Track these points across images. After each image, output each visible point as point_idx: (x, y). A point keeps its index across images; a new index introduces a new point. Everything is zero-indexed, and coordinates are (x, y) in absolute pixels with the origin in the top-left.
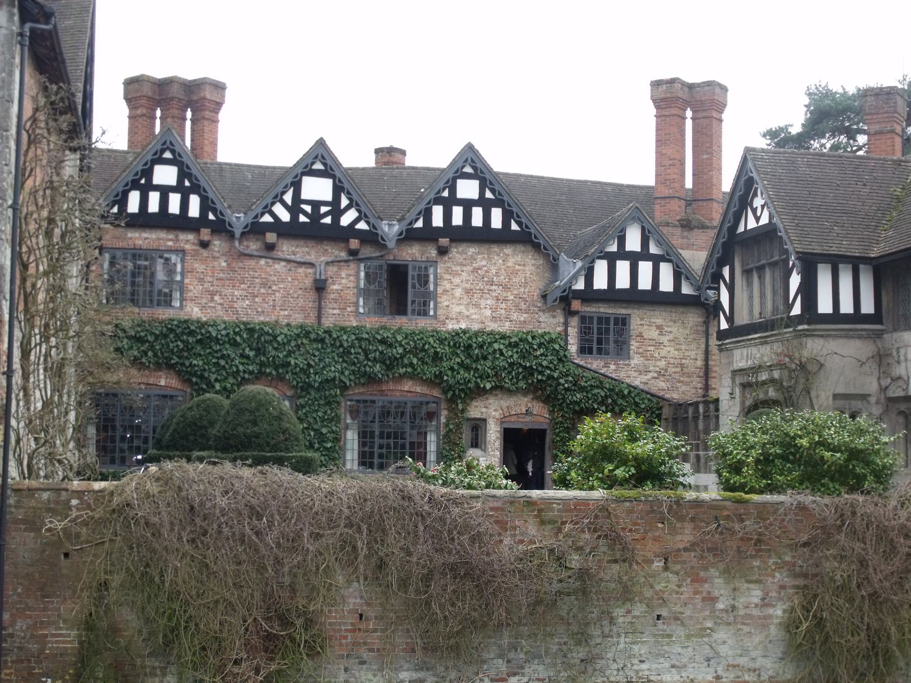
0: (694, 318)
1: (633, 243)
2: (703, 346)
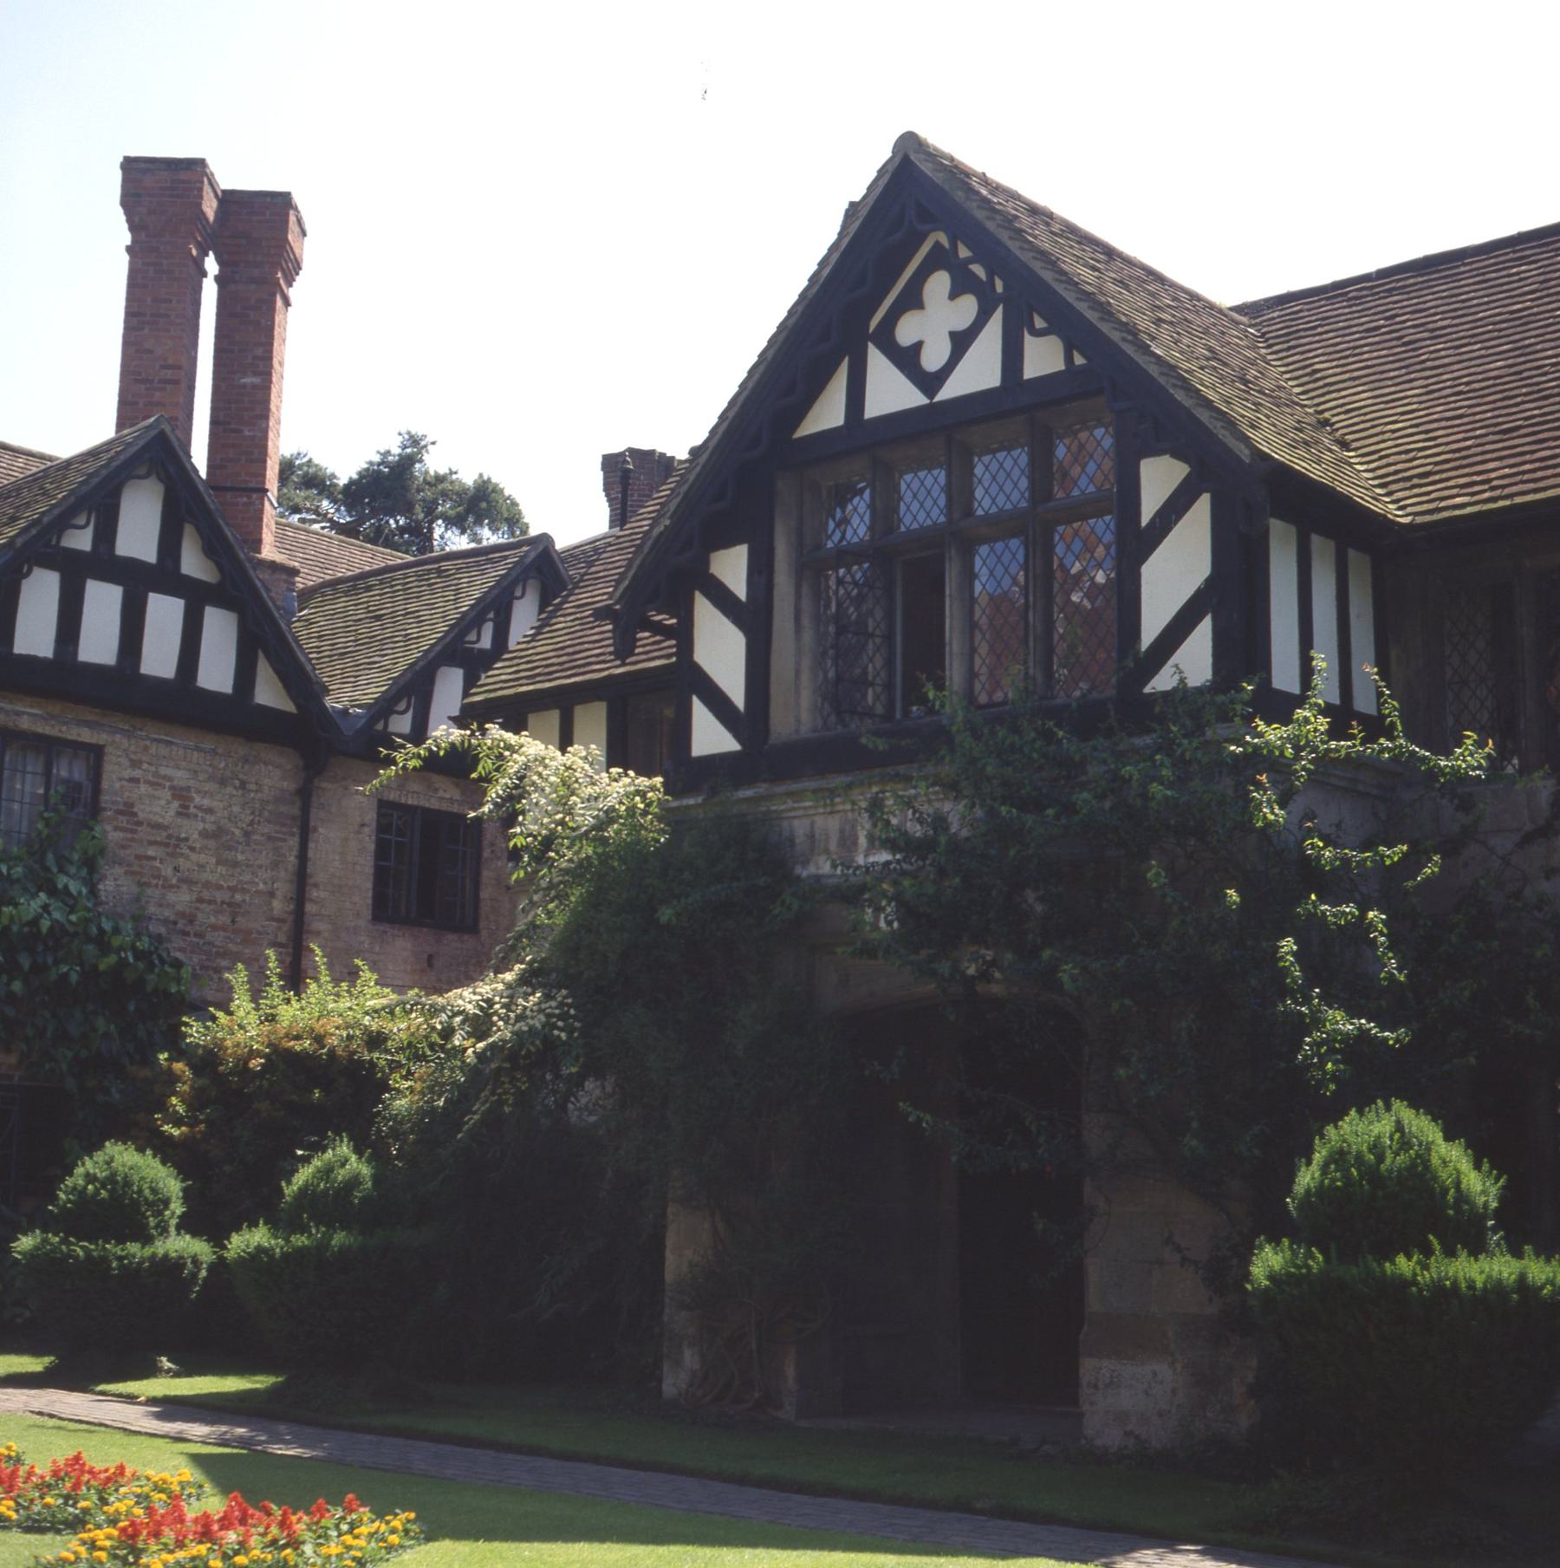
0: (274, 774)
1: (138, 536)
2: (292, 859)
